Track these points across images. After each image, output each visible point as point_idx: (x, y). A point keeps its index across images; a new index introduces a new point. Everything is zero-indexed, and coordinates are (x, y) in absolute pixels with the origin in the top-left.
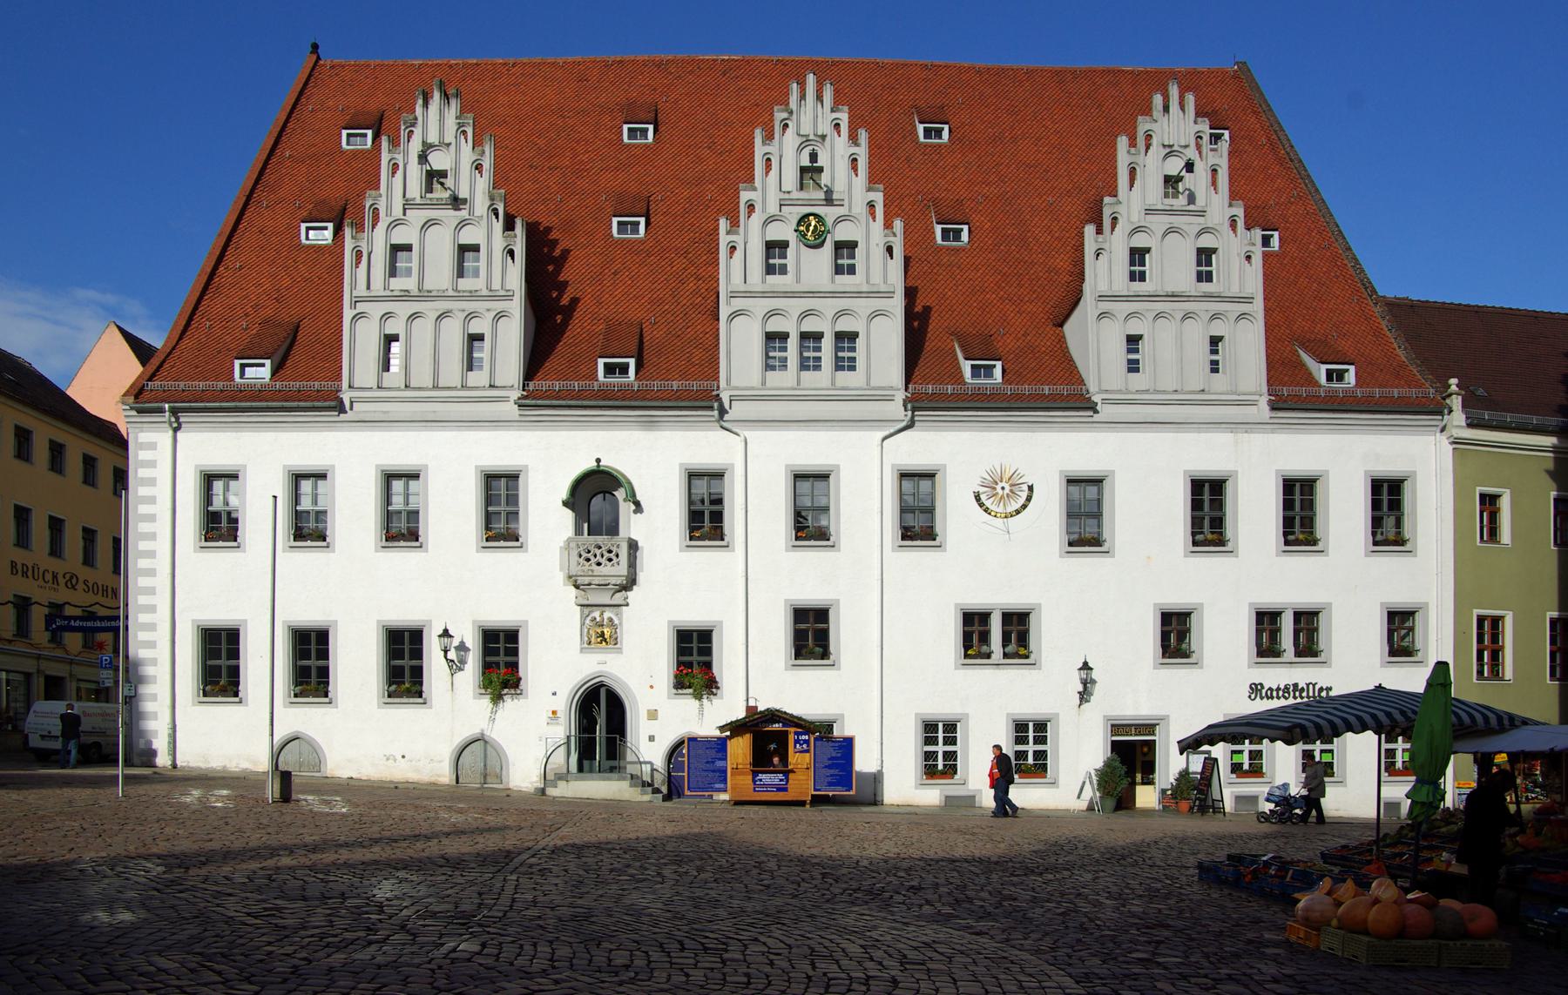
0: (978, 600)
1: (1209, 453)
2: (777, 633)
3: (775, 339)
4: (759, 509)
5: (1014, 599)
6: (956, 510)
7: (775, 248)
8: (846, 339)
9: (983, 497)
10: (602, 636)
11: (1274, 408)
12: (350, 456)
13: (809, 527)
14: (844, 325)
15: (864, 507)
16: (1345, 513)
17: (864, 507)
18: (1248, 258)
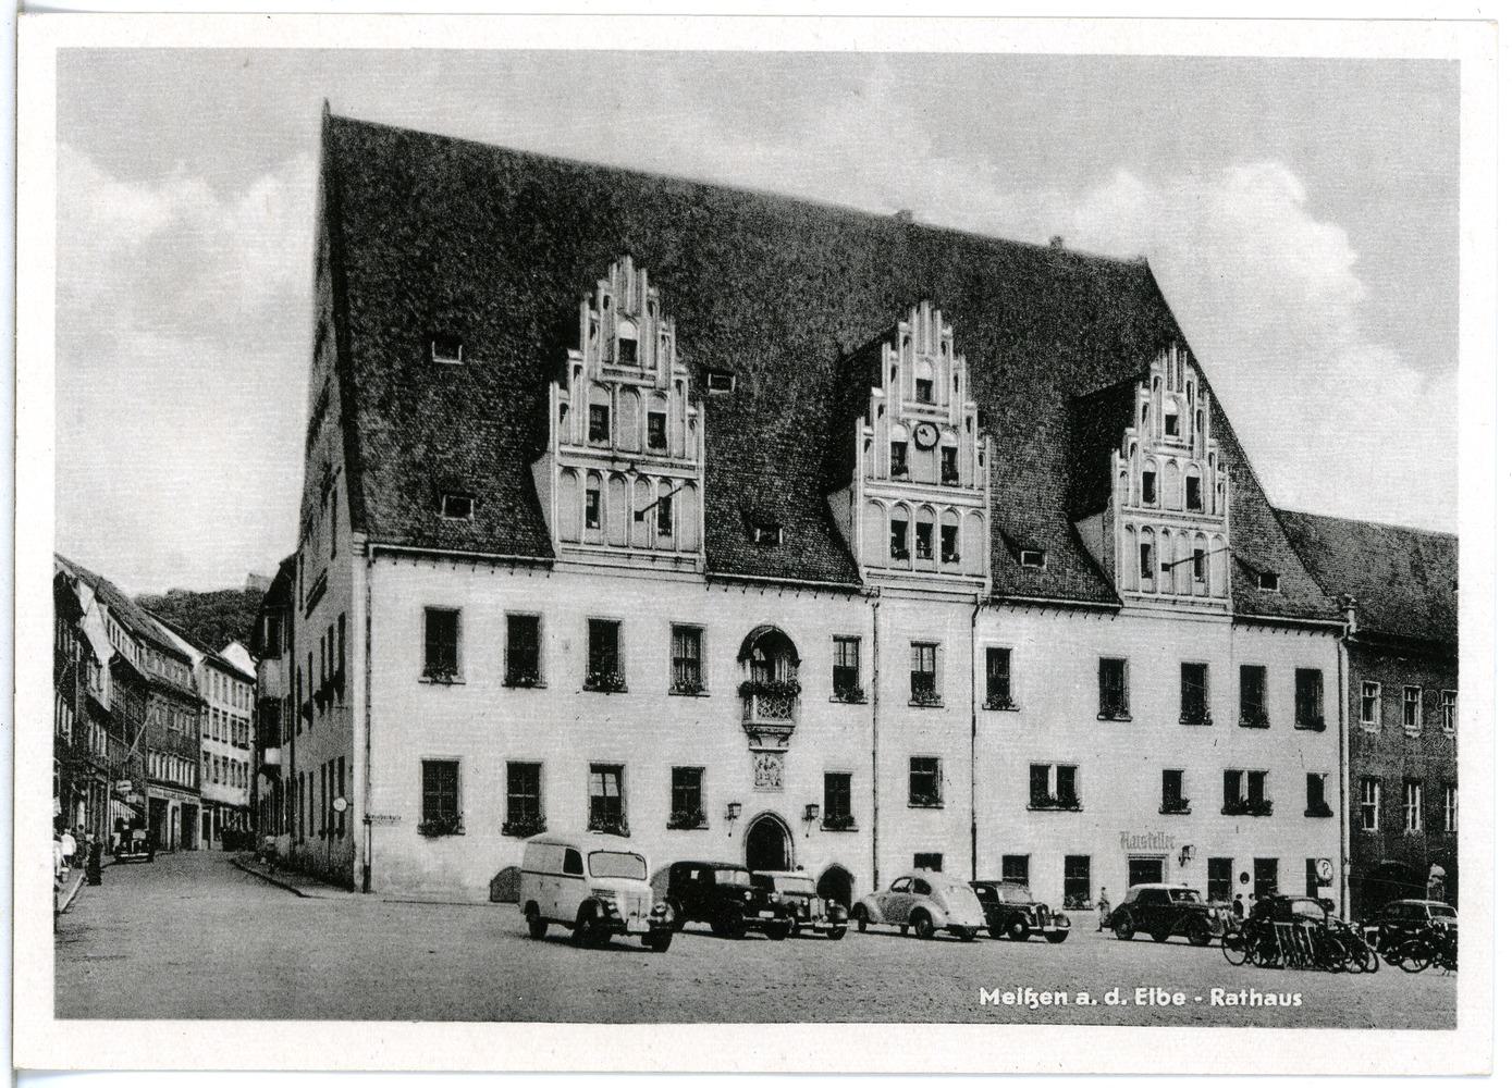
0: (1043, 760)
2: (898, 783)
3: (899, 528)
4: (889, 674)
5: (1068, 760)
7: (899, 449)
8: (950, 533)
10: (768, 776)
12: (564, 603)
13: (924, 687)
15: (961, 679)
16: (1280, 698)
17: (961, 679)
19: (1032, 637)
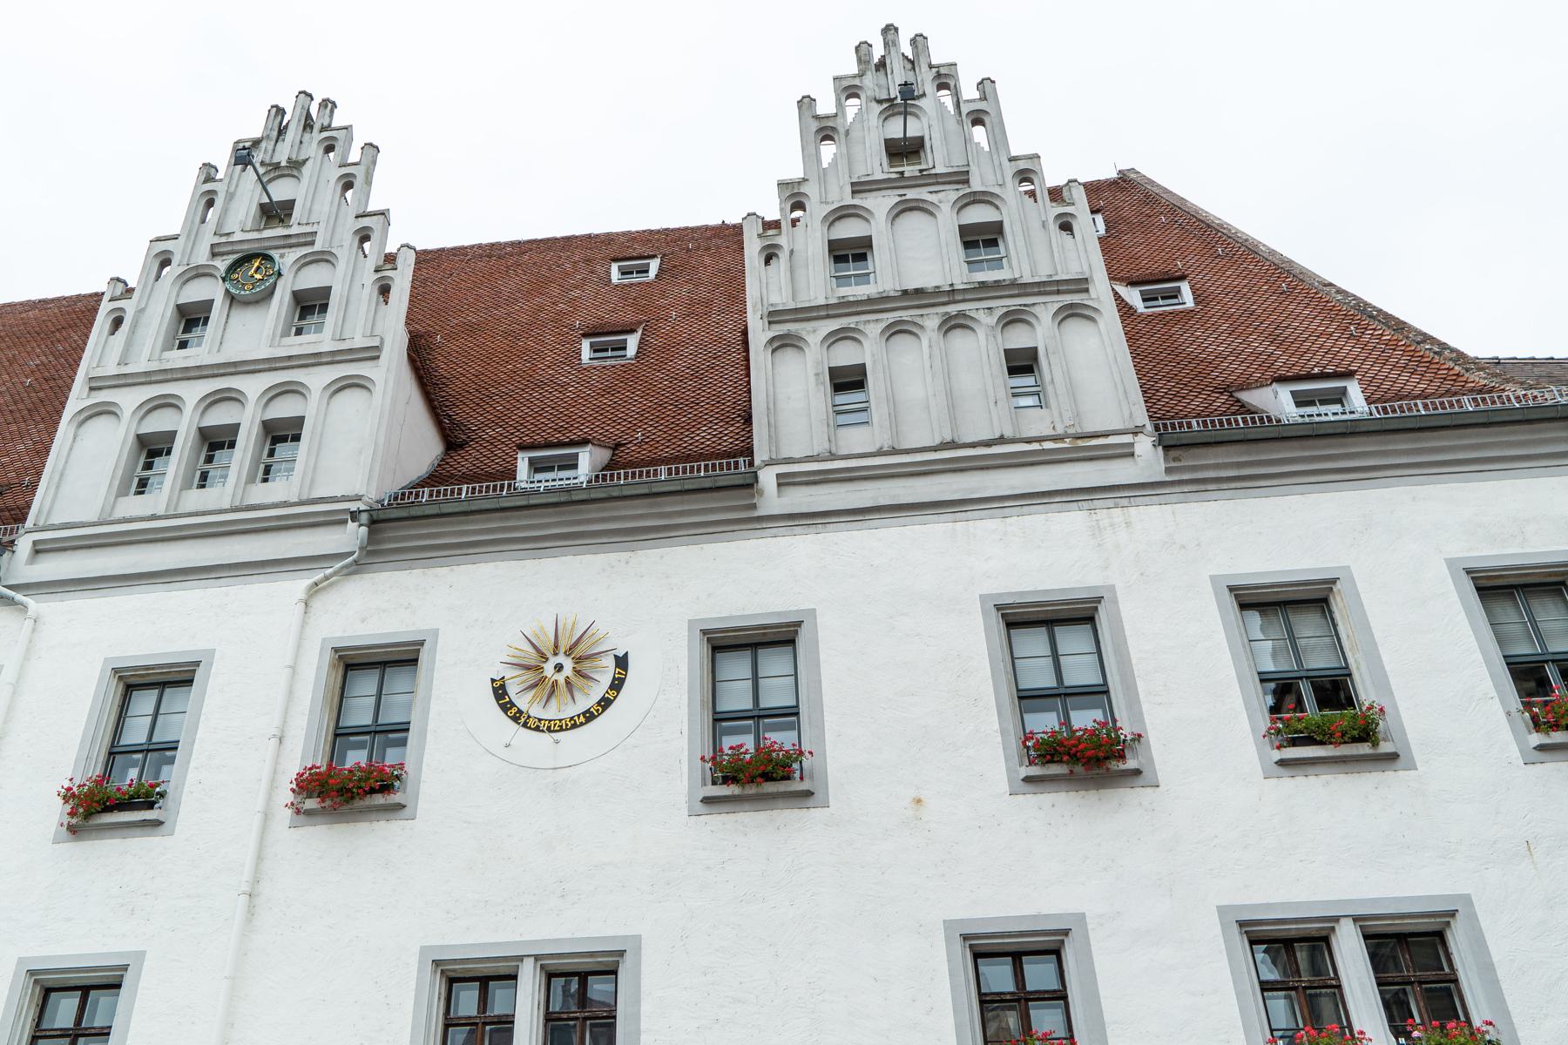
1: (1046, 553)
6: (452, 728)
9: (512, 690)
11: (1170, 445)
14: (284, 409)
18: (1066, 227)
19: (473, 610)
